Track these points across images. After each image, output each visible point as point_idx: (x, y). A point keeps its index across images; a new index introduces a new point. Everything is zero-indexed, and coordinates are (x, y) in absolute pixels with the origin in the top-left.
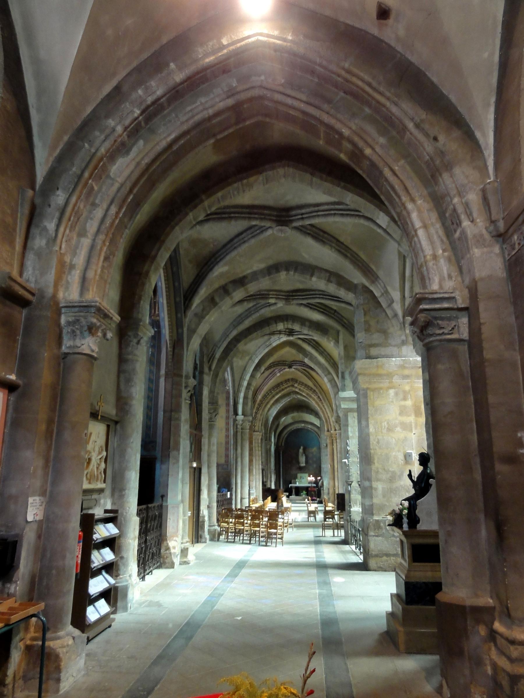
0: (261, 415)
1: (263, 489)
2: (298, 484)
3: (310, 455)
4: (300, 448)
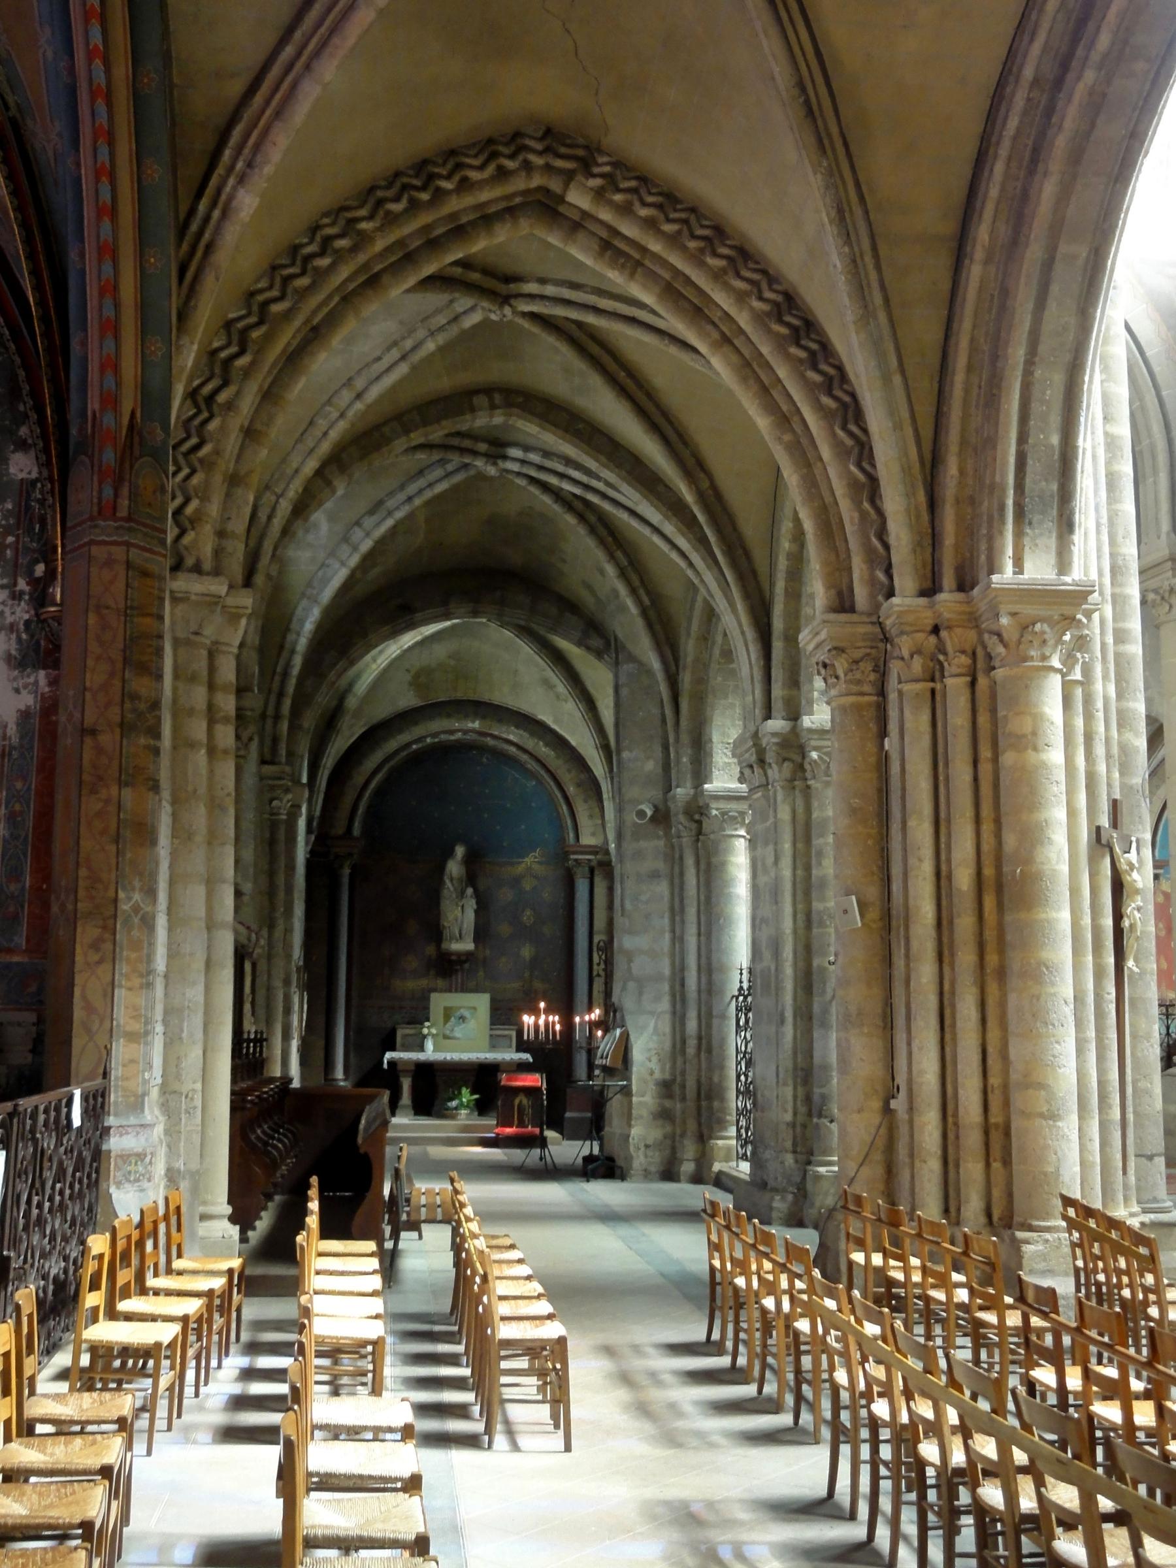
0: (250, 434)
2: (430, 1053)
3: (506, 895)
4: (450, 853)
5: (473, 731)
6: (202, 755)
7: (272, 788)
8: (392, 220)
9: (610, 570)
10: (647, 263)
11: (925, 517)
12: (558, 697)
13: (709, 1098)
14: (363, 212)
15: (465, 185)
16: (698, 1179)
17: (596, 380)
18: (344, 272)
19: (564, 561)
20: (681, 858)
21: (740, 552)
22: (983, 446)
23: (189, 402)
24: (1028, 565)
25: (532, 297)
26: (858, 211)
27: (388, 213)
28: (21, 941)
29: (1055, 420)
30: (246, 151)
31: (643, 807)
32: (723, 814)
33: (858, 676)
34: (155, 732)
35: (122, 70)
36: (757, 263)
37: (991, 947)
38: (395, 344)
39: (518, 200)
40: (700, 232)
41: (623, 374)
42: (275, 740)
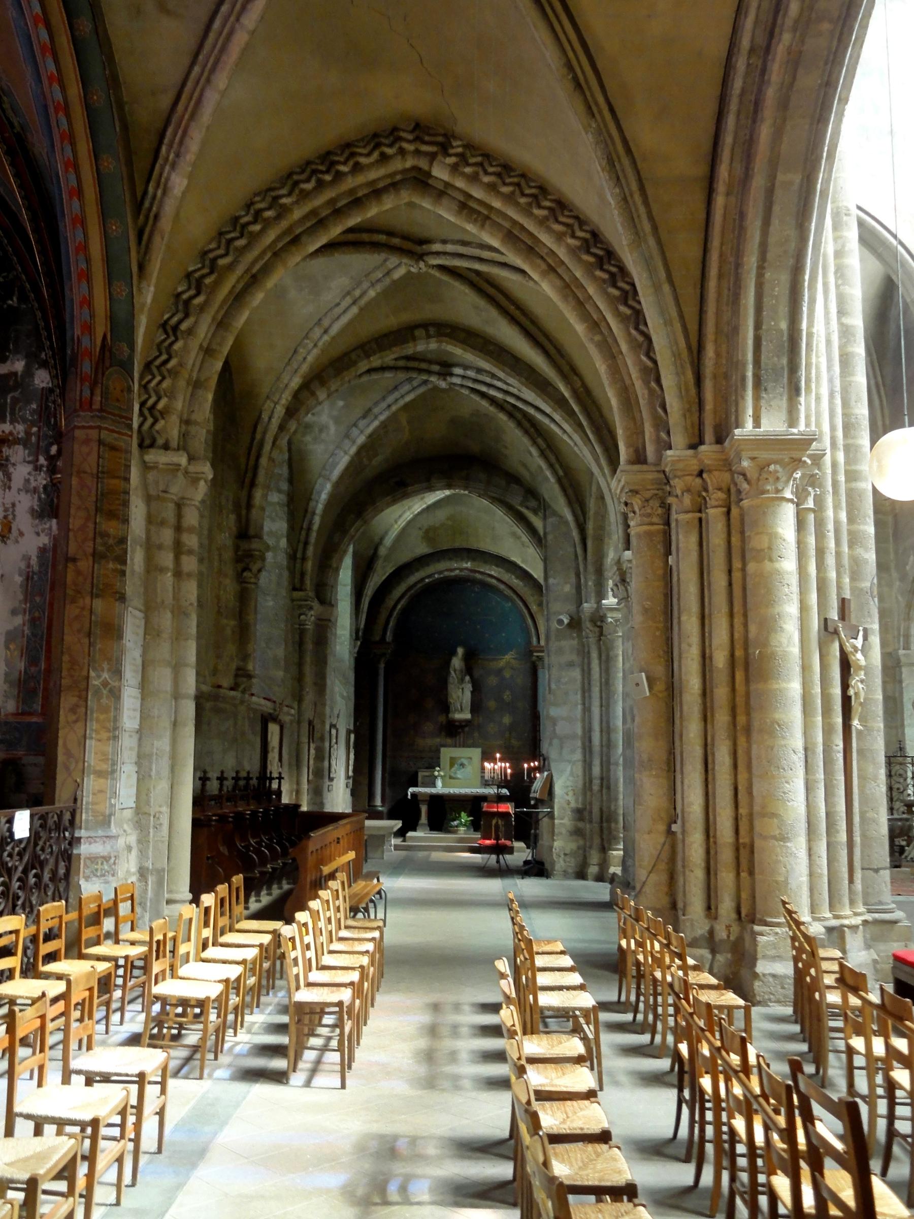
1: (197, 824)
2: (440, 788)
3: (492, 681)
4: (454, 653)
5: (466, 569)
6: (169, 577)
7: (300, 607)
8: (305, 196)
9: (534, 451)
10: (493, 216)
11: (693, 391)
12: (523, 545)
13: (609, 821)
14: (284, 191)
15: (357, 168)
16: (600, 878)
17: (494, 313)
18: (271, 236)
19: (506, 447)
20: (589, 652)
21: (605, 432)
22: (731, 333)
23: (161, 330)
24: (764, 421)
25: (438, 253)
26: (626, 162)
27: (302, 191)
28: (38, 707)
29: (784, 310)
30: (175, 146)
31: (561, 617)
32: (616, 621)
33: (649, 511)
34: (122, 559)
35: (74, 91)
36: (571, 211)
37: (740, 710)
38: (348, 293)
39: (398, 177)
40: (527, 191)
41: (512, 307)
42: (303, 574)
